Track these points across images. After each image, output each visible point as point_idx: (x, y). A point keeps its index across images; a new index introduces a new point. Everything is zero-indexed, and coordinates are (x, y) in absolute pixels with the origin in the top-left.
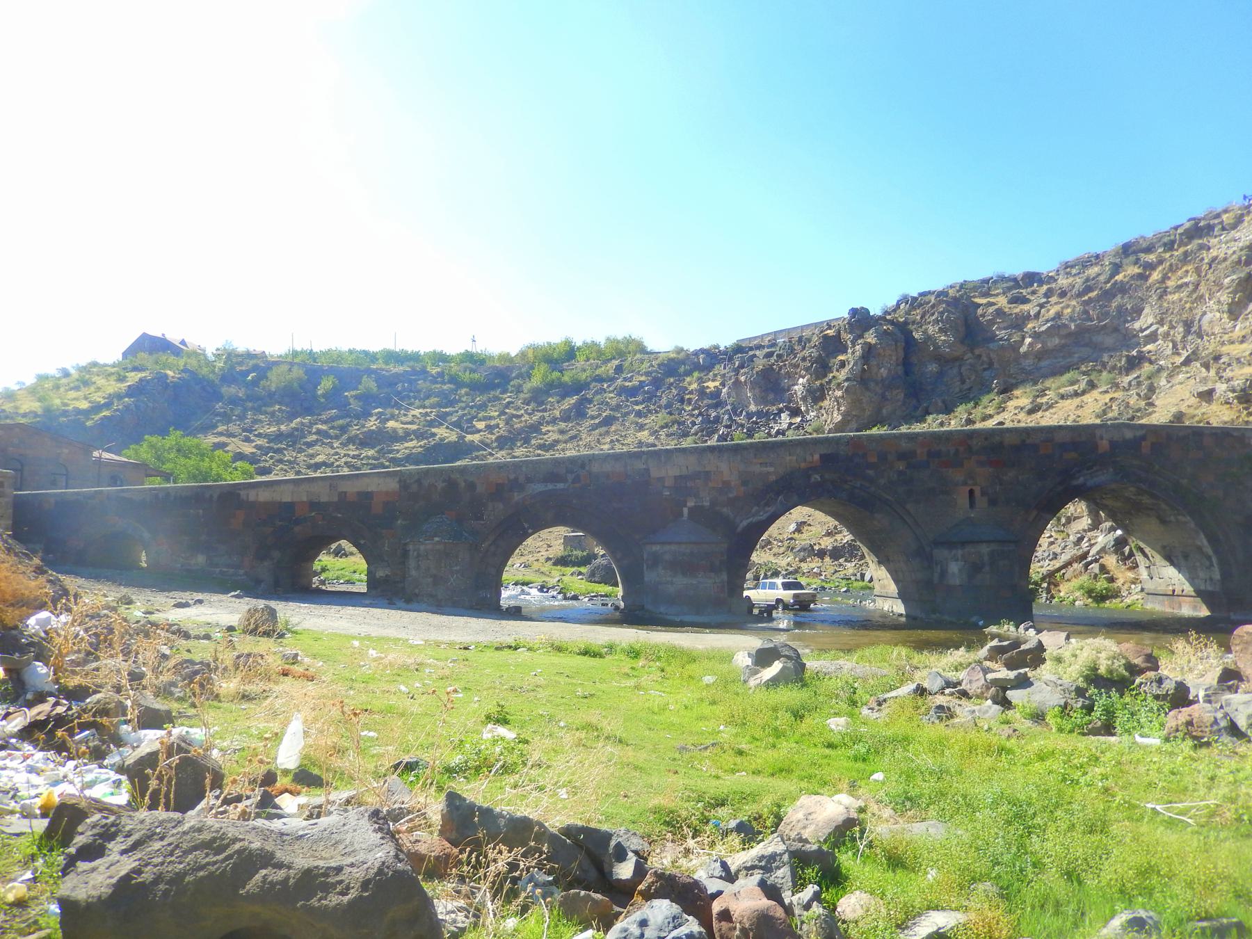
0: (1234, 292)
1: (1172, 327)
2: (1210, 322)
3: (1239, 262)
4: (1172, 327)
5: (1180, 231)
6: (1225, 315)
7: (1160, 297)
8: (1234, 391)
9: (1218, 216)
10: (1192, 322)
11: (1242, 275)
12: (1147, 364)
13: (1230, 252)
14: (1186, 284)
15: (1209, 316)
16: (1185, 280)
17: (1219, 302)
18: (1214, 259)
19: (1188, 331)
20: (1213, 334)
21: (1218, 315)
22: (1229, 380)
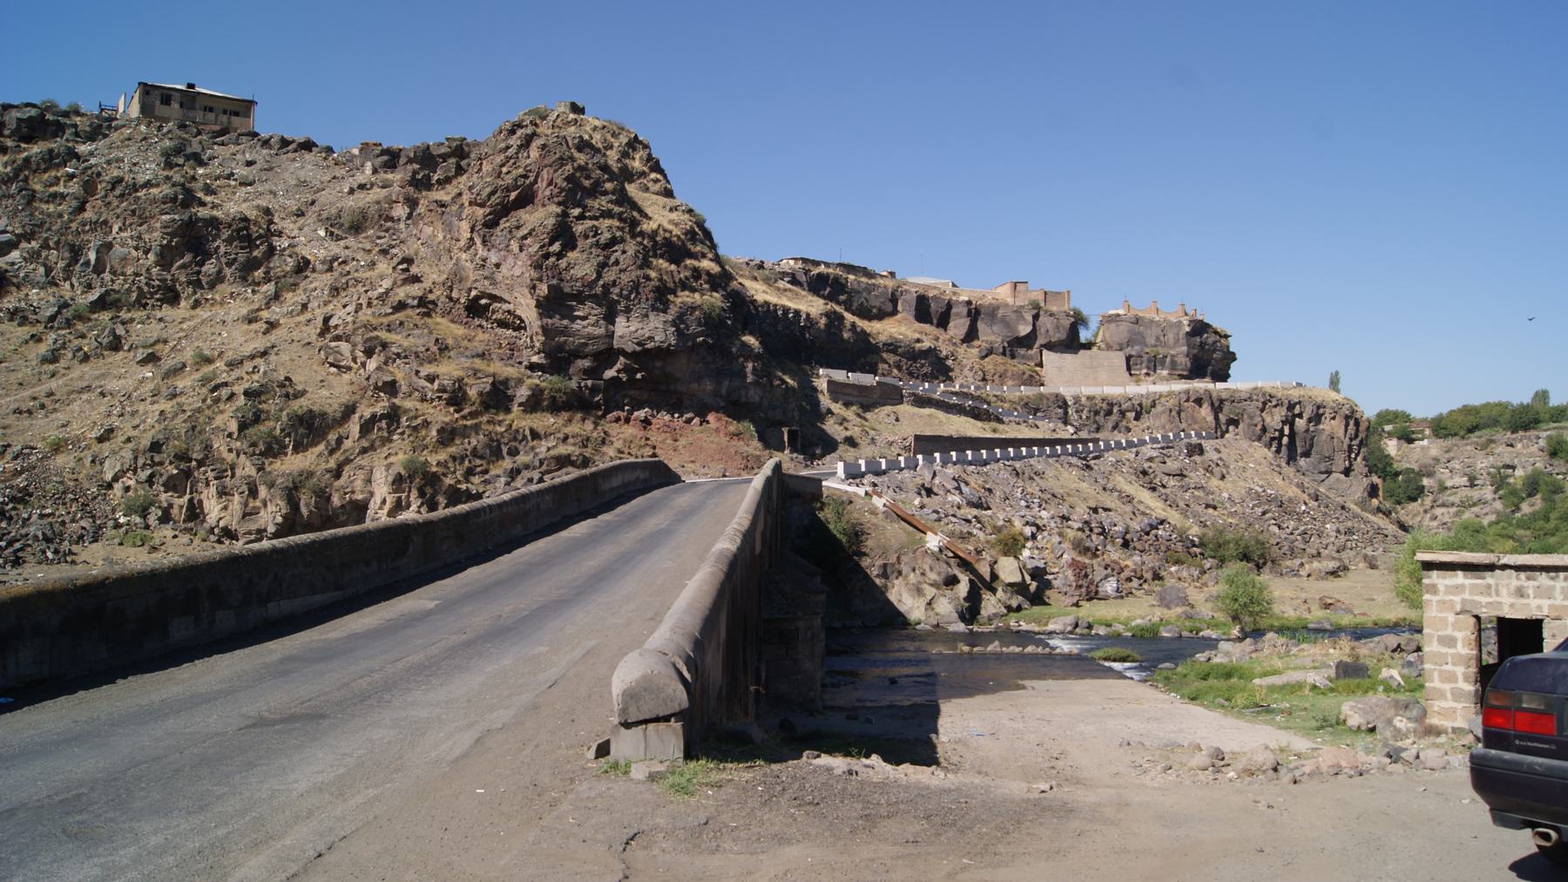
0: (173, 235)
1: (45, 246)
2: (124, 259)
3: (174, 199)
4: (45, 246)
5: (15, 114)
6: (151, 256)
7: (29, 203)
8: (444, 391)
9: (66, 114)
10: (81, 248)
11: (185, 217)
12: (13, 289)
13: (142, 178)
14: (63, 196)
15: (118, 250)
16: (60, 189)
17: (140, 238)
18: (120, 180)
19: (74, 260)
20: (123, 274)
21: (134, 253)
22: (431, 379)
